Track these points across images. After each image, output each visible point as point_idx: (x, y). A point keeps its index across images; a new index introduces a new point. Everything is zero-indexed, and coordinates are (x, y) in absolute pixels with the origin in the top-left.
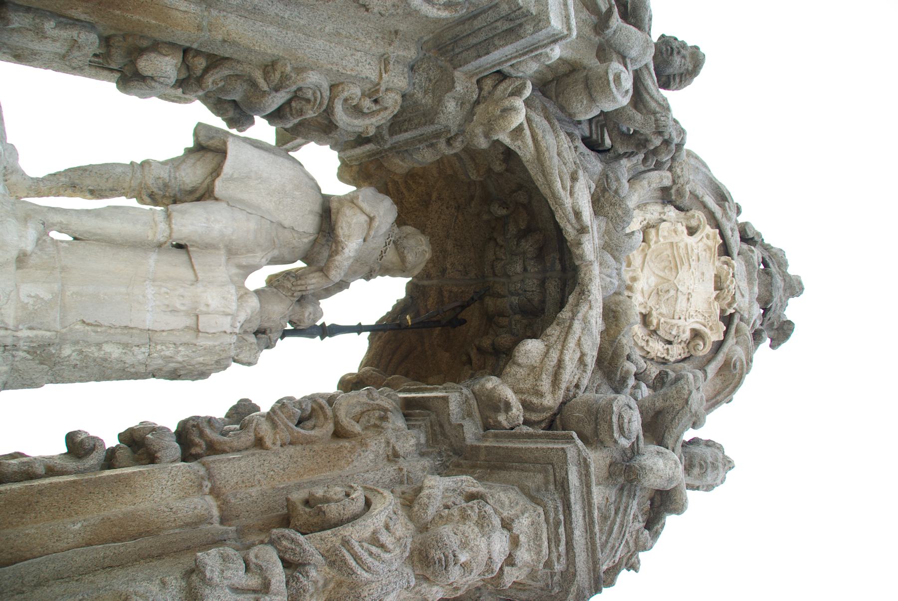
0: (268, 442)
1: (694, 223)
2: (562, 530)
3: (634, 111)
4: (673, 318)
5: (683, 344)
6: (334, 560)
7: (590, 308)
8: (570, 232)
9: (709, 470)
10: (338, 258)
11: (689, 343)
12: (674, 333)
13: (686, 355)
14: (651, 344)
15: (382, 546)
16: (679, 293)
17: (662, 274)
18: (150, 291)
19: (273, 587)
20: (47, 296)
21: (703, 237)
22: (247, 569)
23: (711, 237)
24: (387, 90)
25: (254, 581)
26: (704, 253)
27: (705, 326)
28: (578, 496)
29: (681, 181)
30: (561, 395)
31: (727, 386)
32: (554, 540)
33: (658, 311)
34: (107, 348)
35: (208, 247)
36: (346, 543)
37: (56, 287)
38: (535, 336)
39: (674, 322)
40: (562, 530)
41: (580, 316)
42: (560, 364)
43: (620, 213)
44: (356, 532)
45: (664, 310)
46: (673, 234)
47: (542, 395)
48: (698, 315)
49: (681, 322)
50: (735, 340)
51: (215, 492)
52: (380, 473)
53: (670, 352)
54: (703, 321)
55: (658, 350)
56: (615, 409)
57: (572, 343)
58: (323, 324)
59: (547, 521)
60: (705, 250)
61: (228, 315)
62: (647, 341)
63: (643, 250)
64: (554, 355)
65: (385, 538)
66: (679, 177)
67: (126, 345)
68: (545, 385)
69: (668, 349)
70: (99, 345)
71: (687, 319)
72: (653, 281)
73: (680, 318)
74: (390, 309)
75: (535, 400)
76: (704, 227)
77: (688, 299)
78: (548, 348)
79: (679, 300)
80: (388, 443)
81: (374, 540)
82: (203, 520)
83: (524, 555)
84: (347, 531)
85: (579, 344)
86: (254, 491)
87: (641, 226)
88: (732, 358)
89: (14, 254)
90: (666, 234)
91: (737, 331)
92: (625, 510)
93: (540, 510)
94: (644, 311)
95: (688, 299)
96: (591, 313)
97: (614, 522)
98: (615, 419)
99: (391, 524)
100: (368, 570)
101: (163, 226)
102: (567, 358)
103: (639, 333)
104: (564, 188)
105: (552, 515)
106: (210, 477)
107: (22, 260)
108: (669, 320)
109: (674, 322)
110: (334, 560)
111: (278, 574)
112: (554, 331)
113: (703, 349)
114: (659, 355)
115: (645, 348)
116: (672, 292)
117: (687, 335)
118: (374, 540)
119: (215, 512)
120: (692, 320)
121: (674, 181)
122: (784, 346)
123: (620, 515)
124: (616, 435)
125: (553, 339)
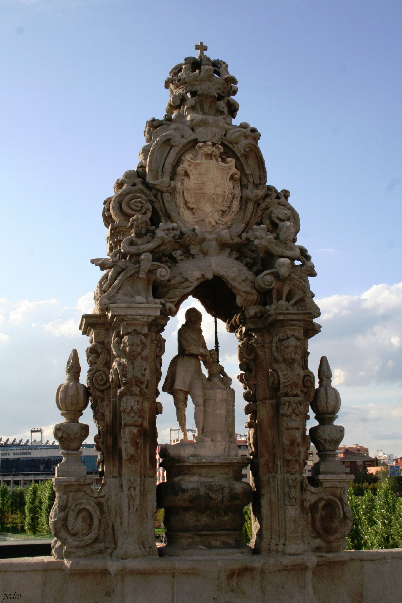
0: (255, 383)
1: (183, 173)
2: (293, 323)
3: (160, 248)
4: (225, 196)
5: (234, 183)
6: (286, 386)
7: (228, 276)
8: (202, 280)
9: (289, 238)
10: (204, 353)
11: (234, 180)
12: (230, 196)
13: (239, 182)
14: (234, 210)
15: (286, 374)
16: (215, 193)
17: (206, 200)
18: (218, 412)
19: (289, 400)
20: (219, 436)
21: (190, 170)
22: (284, 405)
23: (190, 163)
24: (156, 340)
25: (287, 404)
26: (197, 170)
27: (228, 174)
28: (286, 316)
29: (169, 189)
30: (254, 291)
31: (255, 151)
32: (295, 325)
33: (221, 203)
34: (230, 421)
35: (204, 395)
36: (284, 383)
37: (218, 433)
38: (235, 299)
39: (226, 197)
40: (293, 323)
41: (231, 282)
42: (246, 292)
43: (188, 239)
44: (282, 380)
45: (220, 200)
46: (190, 192)
47: (253, 300)
48: (224, 177)
49: (227, 191)
50: (235, 145)
51: (265, 399)
52: (267, 354)
53: (237, 196)
54: (226, 175)
55: (236, 205)
56: (263, 286)
57: (239, 287)
58: (215, 347)
59: (290, 326)
60: (196, 169)
61: (223, 392)
62: (232, 211)
63: (196, 210)
64: (242, 294)
65: (285, 373)
66: (167, 190)
67: (229, 417)
68: (250, 298)
69: (236, 197)
70: (230, 423)
71: (226, 187)
72: (208, 205)
73: (225, 192)
74: (203, 306)
75: (255, 301)
76: (184, 167)
77: (217, 186)
78: (239, 294)
79: (217, 192)
80: (259, 347)
81: (285, 376)
82: (272, 404)
83: (296, 334)
84: (281, 382)
85: (240, 283)
86: (267, 391)
87: (186, 210)
88: (244, 154)
89: (212, 443)
90: (190, 196)
91: (231, 143)
92: (293, 279)
93: (287, 327)
94: (220, 213)
95: (217, 186)
96: (230, 277)
97: (296, 283)
98: (266, 287)
99: (282, 370)
100: (290, 380)
101: (201, 407)
102: (244, 290)
103: (229, 218)
104: (191, 286)
105: (289, 325)
106: (262, 400)
107: (212, 440)
108: (225, 199)
109: (226, 197)
110: (286, 386)
111: (287, 399)
112: (234, 291)
113: (237, 174)
114: (238, 204)
115: (234, 214)
116: (214, 197)
117: (231, 184)
118: (285, 376)
119: (271, 401)
120: (226, 184)
121: (169, 192)
122: (237, 79)
123: (295, 281)
124: (271, 287)
125: (237, 292)
